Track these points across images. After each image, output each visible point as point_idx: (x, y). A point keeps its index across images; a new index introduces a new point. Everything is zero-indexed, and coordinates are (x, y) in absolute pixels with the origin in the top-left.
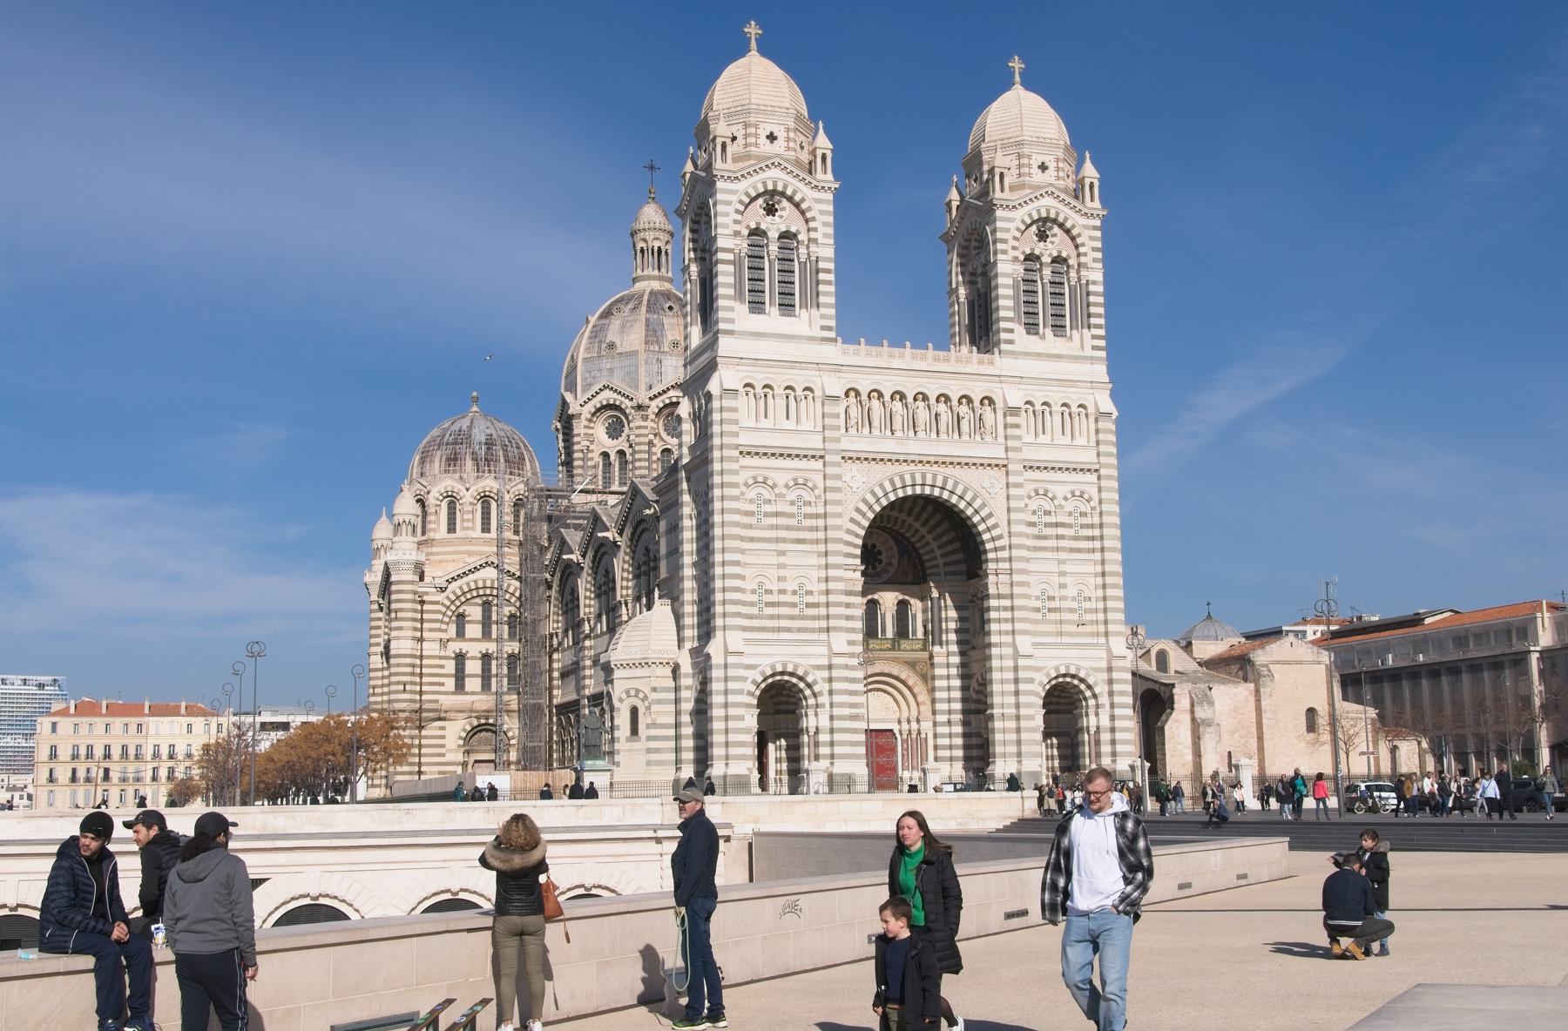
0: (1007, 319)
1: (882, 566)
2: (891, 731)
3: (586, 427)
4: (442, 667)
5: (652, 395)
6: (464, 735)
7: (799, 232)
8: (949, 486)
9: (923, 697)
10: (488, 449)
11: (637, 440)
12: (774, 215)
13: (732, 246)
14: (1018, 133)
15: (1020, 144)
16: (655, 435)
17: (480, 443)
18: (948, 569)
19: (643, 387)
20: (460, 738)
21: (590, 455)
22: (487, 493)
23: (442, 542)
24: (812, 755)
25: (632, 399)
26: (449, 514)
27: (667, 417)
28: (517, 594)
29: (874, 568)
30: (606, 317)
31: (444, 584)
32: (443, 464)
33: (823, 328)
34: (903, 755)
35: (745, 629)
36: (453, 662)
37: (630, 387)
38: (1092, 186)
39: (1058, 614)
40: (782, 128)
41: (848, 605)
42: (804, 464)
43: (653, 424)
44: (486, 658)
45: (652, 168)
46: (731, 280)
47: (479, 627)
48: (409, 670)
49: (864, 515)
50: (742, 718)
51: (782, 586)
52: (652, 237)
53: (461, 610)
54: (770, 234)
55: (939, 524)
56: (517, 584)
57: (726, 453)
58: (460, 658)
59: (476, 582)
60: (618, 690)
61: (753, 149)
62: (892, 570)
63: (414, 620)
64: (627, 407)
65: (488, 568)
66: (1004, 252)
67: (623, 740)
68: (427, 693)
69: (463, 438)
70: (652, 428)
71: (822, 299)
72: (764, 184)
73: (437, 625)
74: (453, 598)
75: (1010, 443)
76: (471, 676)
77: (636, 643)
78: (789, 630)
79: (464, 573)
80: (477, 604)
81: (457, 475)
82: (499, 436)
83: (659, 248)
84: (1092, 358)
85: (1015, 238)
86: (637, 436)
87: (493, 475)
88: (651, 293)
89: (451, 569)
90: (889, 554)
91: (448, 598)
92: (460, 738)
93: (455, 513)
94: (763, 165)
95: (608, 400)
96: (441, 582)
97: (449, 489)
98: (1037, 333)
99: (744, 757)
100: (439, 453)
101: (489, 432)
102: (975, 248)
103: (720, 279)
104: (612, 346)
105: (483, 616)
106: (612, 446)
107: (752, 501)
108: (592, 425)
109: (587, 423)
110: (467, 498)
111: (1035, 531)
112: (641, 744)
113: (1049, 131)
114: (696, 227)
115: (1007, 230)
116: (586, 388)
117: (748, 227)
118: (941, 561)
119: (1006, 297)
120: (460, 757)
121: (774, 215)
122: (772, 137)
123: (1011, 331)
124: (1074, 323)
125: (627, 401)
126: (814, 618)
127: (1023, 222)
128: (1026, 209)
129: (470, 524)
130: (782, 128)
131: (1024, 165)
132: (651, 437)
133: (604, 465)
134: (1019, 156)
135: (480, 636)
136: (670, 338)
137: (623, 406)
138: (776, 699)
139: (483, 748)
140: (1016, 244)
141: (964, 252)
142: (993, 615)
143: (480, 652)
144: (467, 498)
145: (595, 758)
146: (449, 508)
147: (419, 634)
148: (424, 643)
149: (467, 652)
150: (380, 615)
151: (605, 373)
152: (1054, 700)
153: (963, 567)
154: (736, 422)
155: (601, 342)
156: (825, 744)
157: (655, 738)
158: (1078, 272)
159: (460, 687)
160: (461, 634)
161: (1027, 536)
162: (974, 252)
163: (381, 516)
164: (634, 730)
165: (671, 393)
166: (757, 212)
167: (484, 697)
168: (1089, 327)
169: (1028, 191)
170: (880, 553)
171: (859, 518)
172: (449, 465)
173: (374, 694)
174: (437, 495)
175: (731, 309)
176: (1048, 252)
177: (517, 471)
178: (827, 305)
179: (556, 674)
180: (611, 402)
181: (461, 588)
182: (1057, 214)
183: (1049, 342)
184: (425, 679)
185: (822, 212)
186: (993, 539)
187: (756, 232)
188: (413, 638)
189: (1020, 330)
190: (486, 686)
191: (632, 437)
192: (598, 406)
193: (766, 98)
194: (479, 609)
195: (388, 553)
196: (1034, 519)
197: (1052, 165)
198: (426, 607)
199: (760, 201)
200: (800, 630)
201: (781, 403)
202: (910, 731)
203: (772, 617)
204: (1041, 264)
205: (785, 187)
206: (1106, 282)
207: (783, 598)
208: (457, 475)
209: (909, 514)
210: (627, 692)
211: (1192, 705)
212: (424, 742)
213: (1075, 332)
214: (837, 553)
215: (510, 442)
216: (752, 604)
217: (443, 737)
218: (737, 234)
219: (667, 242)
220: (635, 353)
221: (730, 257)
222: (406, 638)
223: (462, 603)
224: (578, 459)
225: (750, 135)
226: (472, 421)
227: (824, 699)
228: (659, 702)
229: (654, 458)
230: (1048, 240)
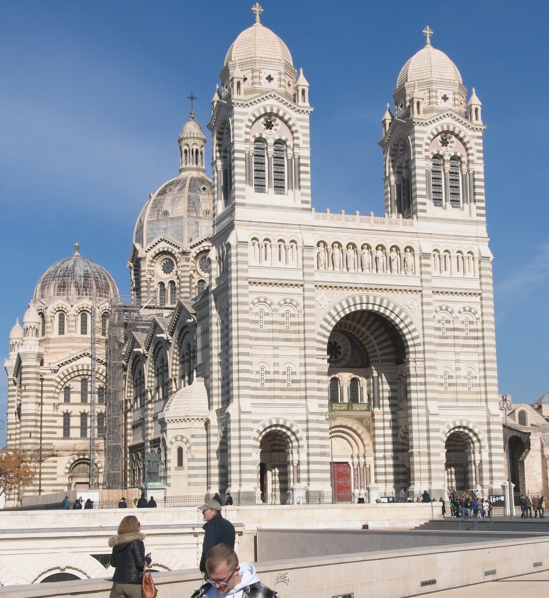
0: (422, 196)
1: (341, 356)
2: (347, 463)
3: (149, 266)
4: (55, 421)
5: (192, 245)
6: (69, 466)
7: (287, 140)
8: (384, 304)
9: (368, 441)
10: (86, 280)
11: (183, 274)
12: (271, 129)
13: (244, 149)
14: (429, 76)
15: (430, 83)
16: (194, 271)
17: (80, 276)
18: (384, 358)
19: (186, 240)
20: (67, 468)
21: (152, 284)
22: (85, 309)
23: (55, 340)
24: (296, 479)
25: (179, 248)
26: (60, 322)
27: (202, 259)
28: (104, 374)
29: (336, 357)
30: (162, 194)
31: (56, 369)
32: (56, 289)
33: (303, 202)
34: (354, 479)
35: (252, 397)
36: (62, 419)
37: (178, 240)
38: (476, 110)
39: (455, 387)
40: (276, 72)
41: (319, 382)
42: (290, 290)
43: (192, 264)
44: (84, 416)
45: (192, 98)
46: (243, 171)
47: (80, 395)
48: (33, 423)
49: (329, 323)
50: (250, 455)
51: (276, 369)
52: (192, 143)
53: (67, 385)
54: (268, 141)
55: (378, 328)
56: (104, 367)
57: (240, 282)
58: (67, 416)
59: (77, 366)
60: (169, 437)
61: (258, 86)
62: (347, 358)
63: (37, 391)
64: (176, 253)
65: (85, 357)
66: (420, 153)
67: (173, 469)
68: (45, 438)
69: (69, 273)
70: (192, 266)
71: (302, 183)
72: (265, 108)
73: (52, 395)
74: (62, 376)
75: (424, 277)
77: (182, 406)
78: (281, 397)
79: (70, 360)
80: (78, 381)
81: (65, 297)
82: (92, 271)
83: (197, 150)
84: (477, 222)
85: (427, 144)
86: (182, 272)
87: (89, 297)
88: (191, 179)
89: (61, 358)
90: (345, 346)
91: (59, 377)
92: (67, 468)
93: (64, 322)
94: (264, 96)
95: (163, 248)
97: (60, 306)
98: (441, 205)
99: (251, 480)
100: (53, 282)
101: (86, 269)
102: (401, 150)
103: (236, 170)
104: (166, 213)
105: (82, 389)
106: (166, 278)
107: (256, 314)
108: (153, 264)
109: (150, 263)
110: (72, 311)
111: (439, 333)
112: (184, 472)
113: (450, 75)
114: (220, 136)
115: (422, 139)
116: (150, 240)
117: (254, 136)
118: (379, 353)
119: (421, 182)
120: (66, 481)
121: (271, 129)
123: (425, 204)
124: (465, 199)
125: (176, 249)
126: (297, 390)
127: (432, 133)
128: (434, 125)
129: (74, 329)
130: (276, 72)
131: (433, 97)
132: (192, 272)
133: (161, 290)
134: (430, 91)
135: (79, 401)
136: (204, 208)
137: (173, 252)
138: (272, 443)
139: (82, 474)
140: (427, 147)
141: (394, 153)
142: (413, 388)
143: (80, 412)
144: (72, 311)
145: (155, 481)
146: (60, 318)
147: (40, 400)
148: (43, 406)
149: (71, 412)
150: (15, 388)
151: (162, 231)
152: (453, 443)
153: (393, 357)
154: (247, 263)
155: (159, 210)
156: (304, 472)
157: (193, 468)
158: (468, 166)
159: (66, 435)
160: (67, 400)
161: (435, 337)
162: (400, 153)
163: (15, 323)
164: (180, 463)
165: (205, 244)
166: (260, 129)
167: (82, 441)
168: (475, 202)
169: (435, 114)
170: (339, 347)
171: (326, 325)
172: (60, 290)
173: (10, 440)
174: (52, 310)
175: (243, 190)
176: (448, 153)
177: (104, 294)
178: (306, 187)
179: (129, 426)
180: (166, 249)
181: (67, 370)
182: (454, 128)
183: (450, 211)
184: (44, 430)
185: (302, 127)
186: (413, 339)
187: (260, 140)
188: (36, 403)
189: (430, 203)
190: (84, 434)
191: (179, 272)
192: (157, 252)
193: (266, 53)
194: (79, 384)
195: (20, 348)
196: (440, 325)
197: (450, 96)
198: (44, 383)
199: (262, 120)
201: (276, 250)
202: (359, 463)
203: (269, 389)
204: (444, 161)
205: (278, 110)
206: (486, 173)
207: (277, 377)
208: (65, 297)
209: (358, 322)
210: (176, 438)
211: (542, 447)
212: (43, 470)
213: (465, 205)
214: (312, 348)
215: (100, 275)
216: (257, 381)
217: (55, 467)
218: (247, 141)
219: (202, 146)
220: (181, 218)
221: (243, 156)
222: (31, 403)
223: (68, 380)
224: (144, 286)
225: (256, 77)
226: (75, 262)
227: (303, 442)
228: (196, 444)
229: (194, 286)
230: (448, 145)
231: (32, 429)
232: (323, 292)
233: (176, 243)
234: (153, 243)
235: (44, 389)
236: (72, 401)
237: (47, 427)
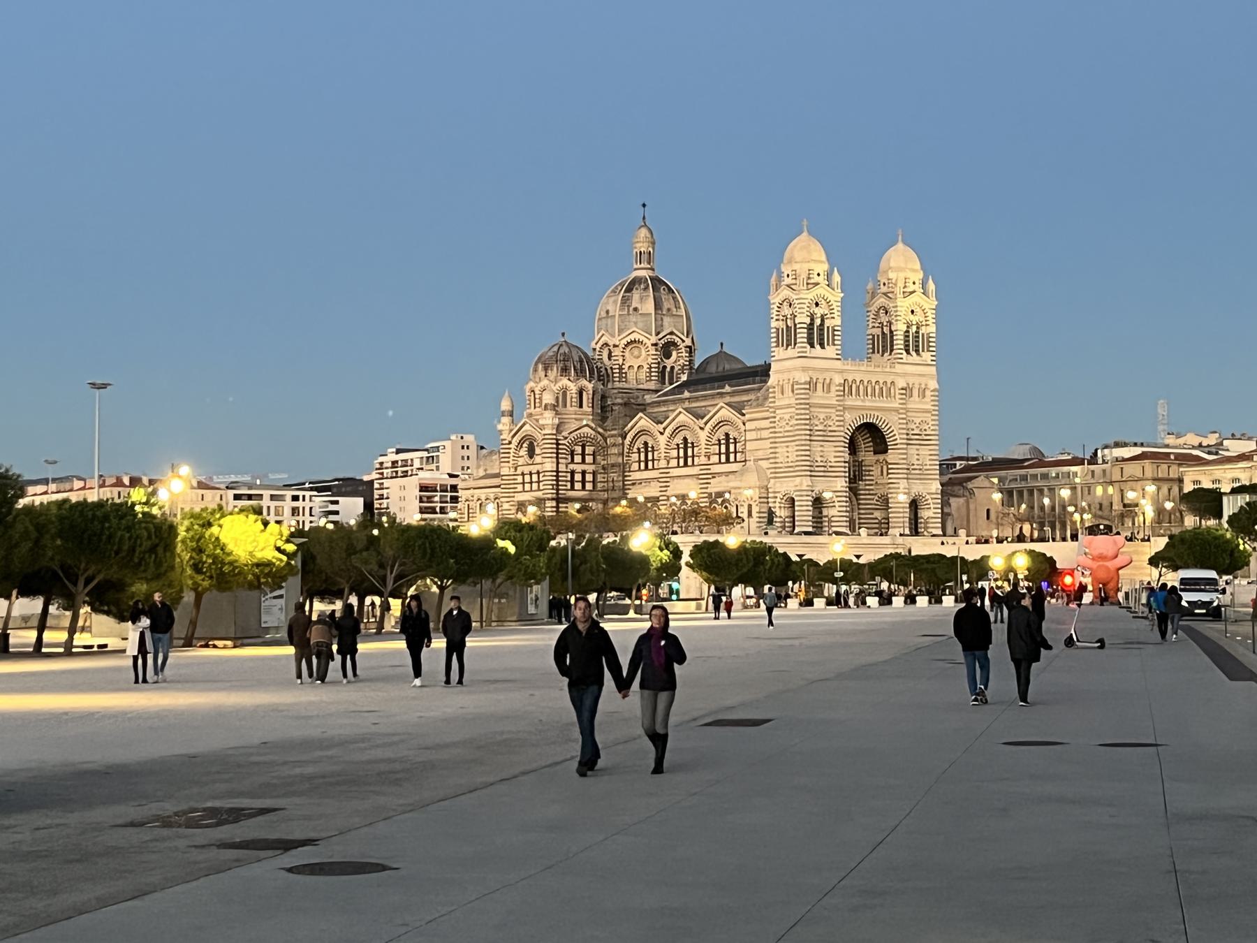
33: (837, 354)
36: (569, 475)
44: (584, 473)
45: (644, 205)
47: (580, 456)
51: (822, 459)
76: (577, 481)
104: (636, 309)
123: (902, 354)
135: (580, 461)
155: (629, 306)
165: (668, 337)
183: (914, 358)
190: (584, 488)
220: (651, 314)
228: (760, 503)
234: (624, 335)
237: (563, 481)
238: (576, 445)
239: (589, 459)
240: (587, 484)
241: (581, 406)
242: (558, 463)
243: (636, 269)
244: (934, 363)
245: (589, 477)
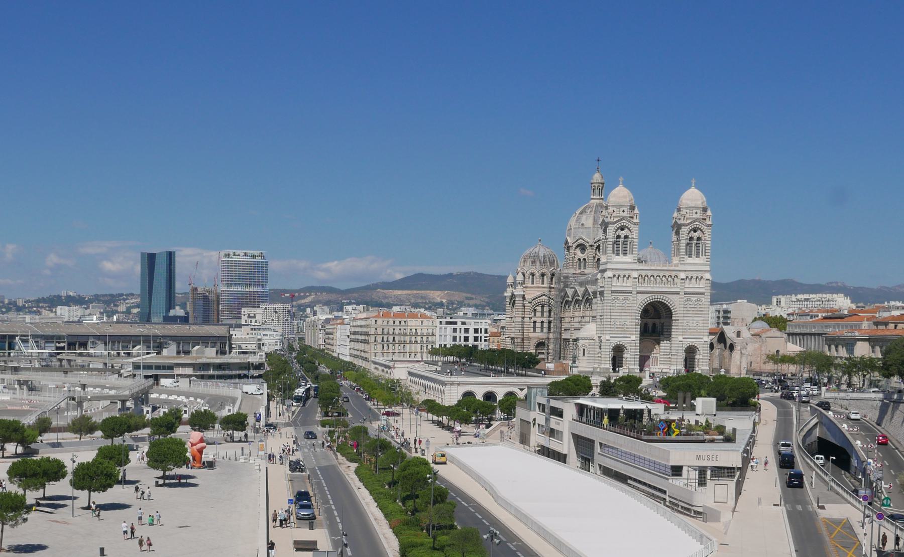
11: (590, 256)
33: (634, 260)
37: (588, 238)
44: (542, 322)
47: (540, 313)
48: (520, 326)
58: (535, 322)
60: (580, 344)
62: (652, 315)
63: (522, 311)
73: (528, 313)
81: (534, 267)
90: (651, 310)
96: (530, 300)
101: (545, 252)
104: (583, 224)
122: (623, 211)
123: (684, 258)
132: (594, 255)
135: (540, 316)
159: (534, 331)
160: (535, 315)
164: (584, 355)
167: (541, 334)
175: (611, 256)
179: (563, 329)
185: (635, 230)
190: (542, 331)
198: (526, 307)
200: (624, 334)
203: (617, 331)
207: (620, 326)
220: (590, 228)
228: (590, 348)
229: (595, 261)
231: (520, 329)
232: (640, 295)
233: (588, 240)
235: (525, 310)
236: (537, 316)
237: (526, 327)
238: (537, 306)
239: (546, 314)
240: (544, 329)
241: (543, 283)
242: (523, 318)
243: (592, 199)
244: (709, 263)
245: (545, 325)
